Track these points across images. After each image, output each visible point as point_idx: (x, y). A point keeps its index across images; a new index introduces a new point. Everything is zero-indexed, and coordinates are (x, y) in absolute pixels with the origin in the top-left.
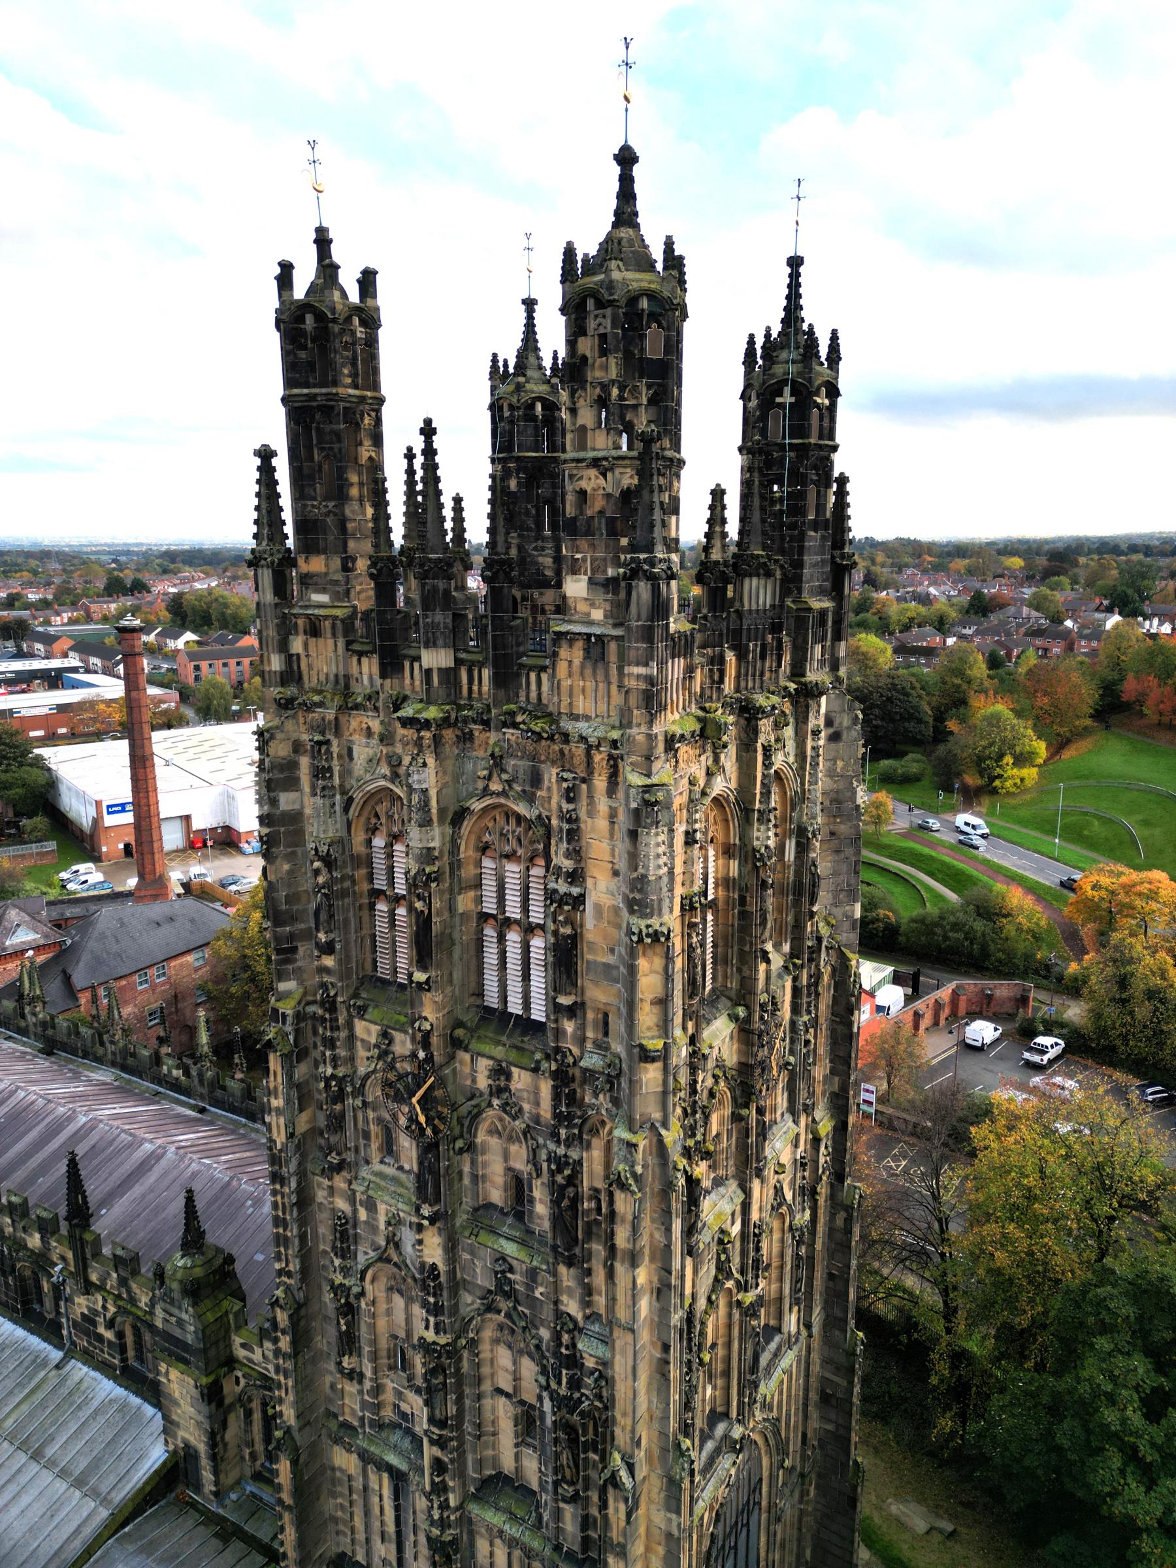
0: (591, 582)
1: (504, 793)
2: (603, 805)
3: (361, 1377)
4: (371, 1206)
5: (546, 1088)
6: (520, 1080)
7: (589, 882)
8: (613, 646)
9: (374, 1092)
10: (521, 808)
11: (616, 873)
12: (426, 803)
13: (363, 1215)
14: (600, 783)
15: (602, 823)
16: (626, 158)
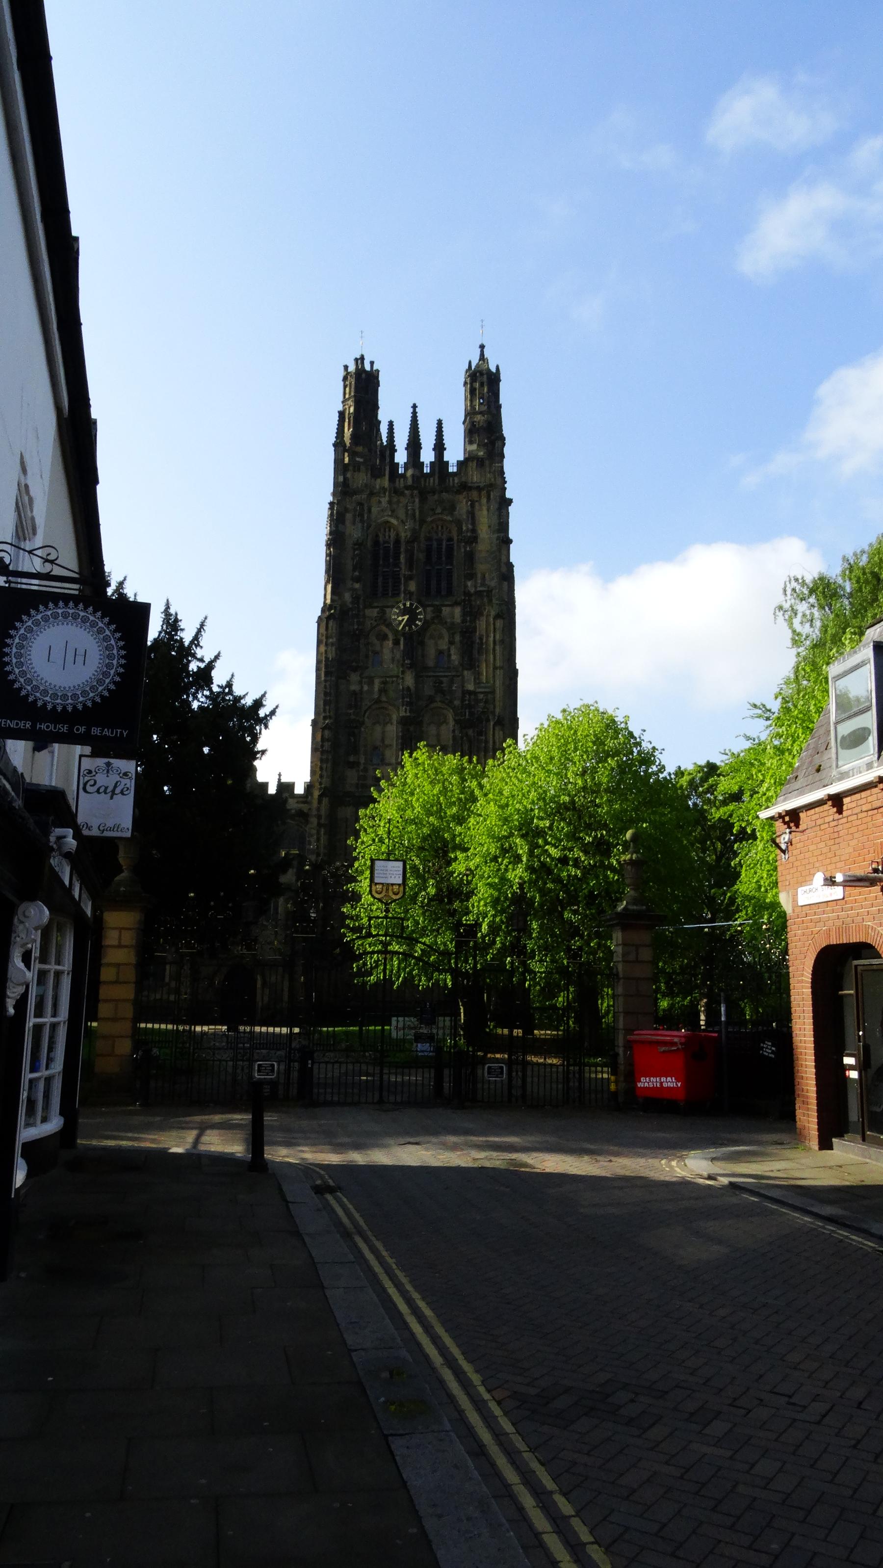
0: (479, 445)
1: (441, 513)
2: (485, 508)
3: (358, 764)
4: (371, 683)
5: (458, 611)
6: (446, 611)
7: (479, 532)
8: (487, 462)
9: (373, 639)
10: (449, 518)
11: (489, 527)
12: (414, 515)
13: (366, 688)
14: (484, 501)
15: (485, 512)
16: (482, 347)
